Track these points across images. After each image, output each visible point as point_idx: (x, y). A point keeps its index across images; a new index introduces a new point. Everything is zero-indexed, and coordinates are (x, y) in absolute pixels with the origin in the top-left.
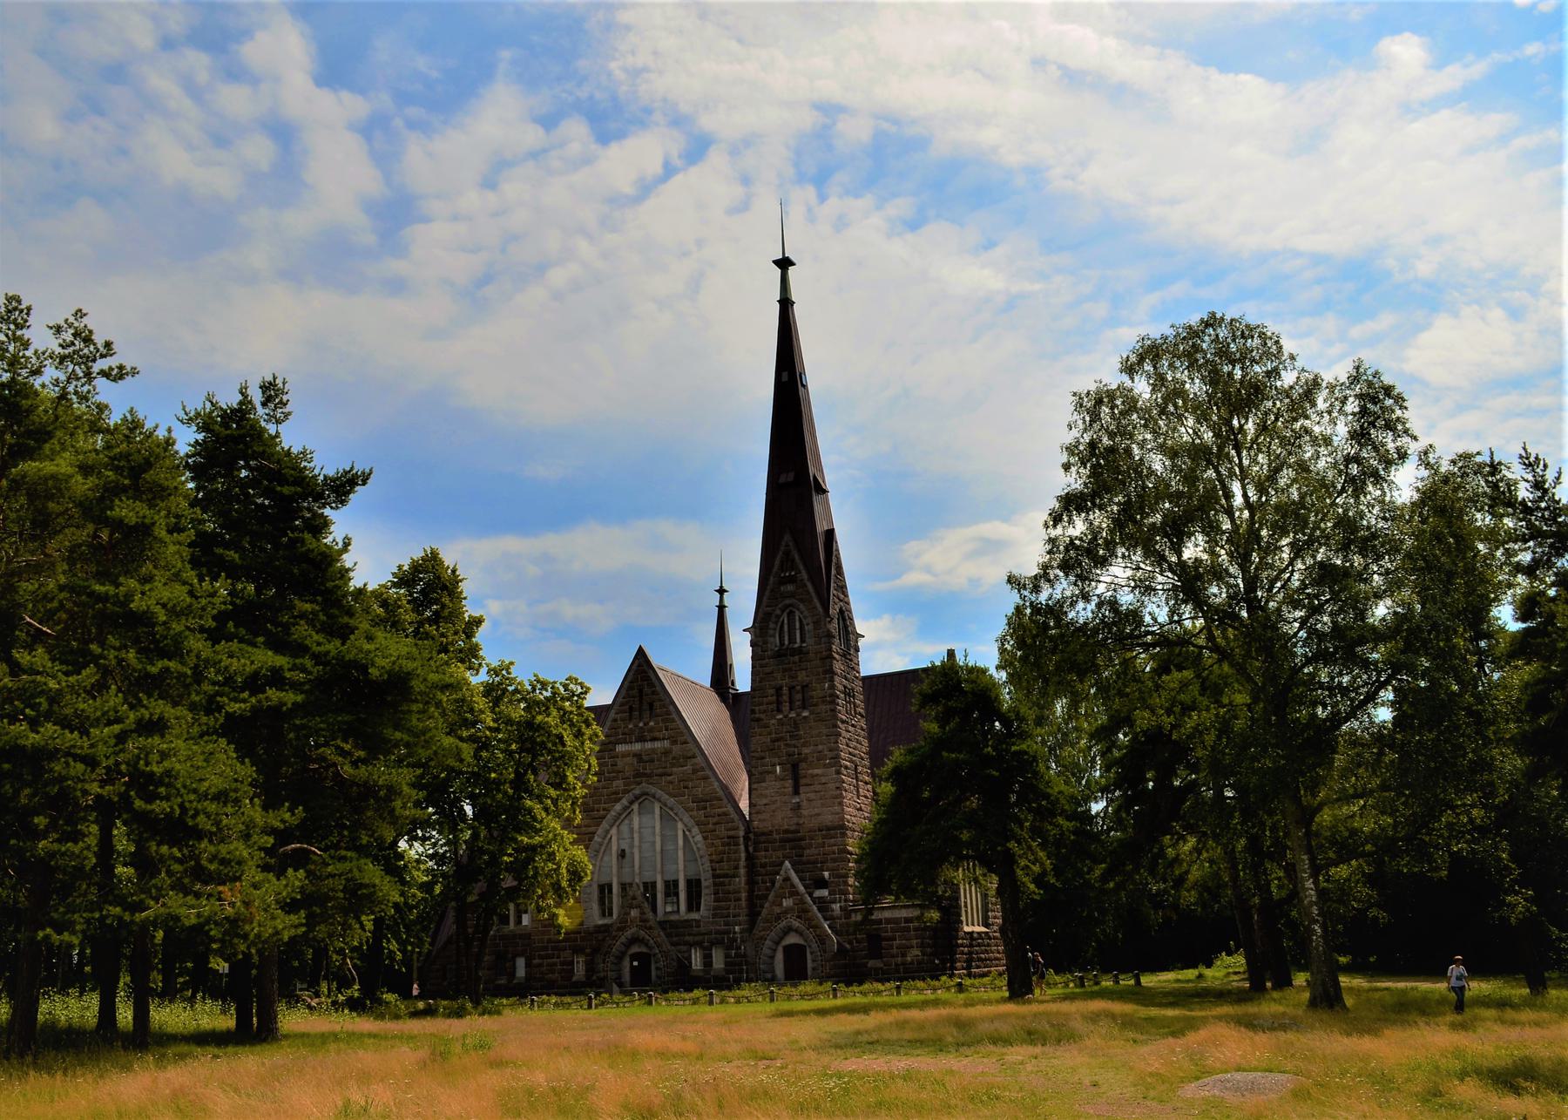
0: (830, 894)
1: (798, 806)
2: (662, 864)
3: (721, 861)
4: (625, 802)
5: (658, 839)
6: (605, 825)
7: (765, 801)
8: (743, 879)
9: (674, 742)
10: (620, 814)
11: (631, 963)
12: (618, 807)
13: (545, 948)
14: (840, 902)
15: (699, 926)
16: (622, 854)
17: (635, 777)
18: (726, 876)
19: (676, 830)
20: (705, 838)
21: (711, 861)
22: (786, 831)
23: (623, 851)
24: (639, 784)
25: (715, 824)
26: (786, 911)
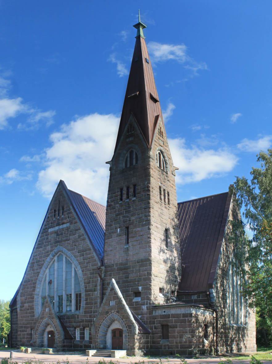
0: (141, 300)
1: (127, 249)
2: (66, 287)
3: (89, 283)
4: (51, 256)
5: (64, 273)
6: (43, 268)
7: (111, 248)
8: (99, 291)
9: (71, 223)
10: (50, 262)
11: (48, 336)
12: (48, 259)
13: (22, 327)
14: (147, 304)
15: (78, 318)
16: (50, 282)
17: (55, 243)
18: (91, 291)
19: (71, 267)
20: (83, 271)
21: (85, 283)
22: (121, 264)
23: (51, 280)
24: (56, 246)
25: (87, 263)
26: (112, 308)
